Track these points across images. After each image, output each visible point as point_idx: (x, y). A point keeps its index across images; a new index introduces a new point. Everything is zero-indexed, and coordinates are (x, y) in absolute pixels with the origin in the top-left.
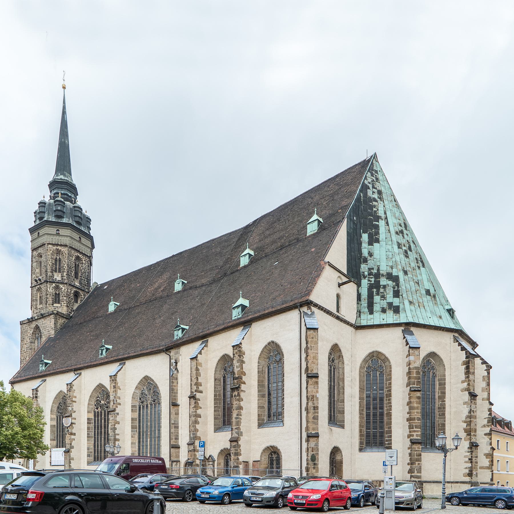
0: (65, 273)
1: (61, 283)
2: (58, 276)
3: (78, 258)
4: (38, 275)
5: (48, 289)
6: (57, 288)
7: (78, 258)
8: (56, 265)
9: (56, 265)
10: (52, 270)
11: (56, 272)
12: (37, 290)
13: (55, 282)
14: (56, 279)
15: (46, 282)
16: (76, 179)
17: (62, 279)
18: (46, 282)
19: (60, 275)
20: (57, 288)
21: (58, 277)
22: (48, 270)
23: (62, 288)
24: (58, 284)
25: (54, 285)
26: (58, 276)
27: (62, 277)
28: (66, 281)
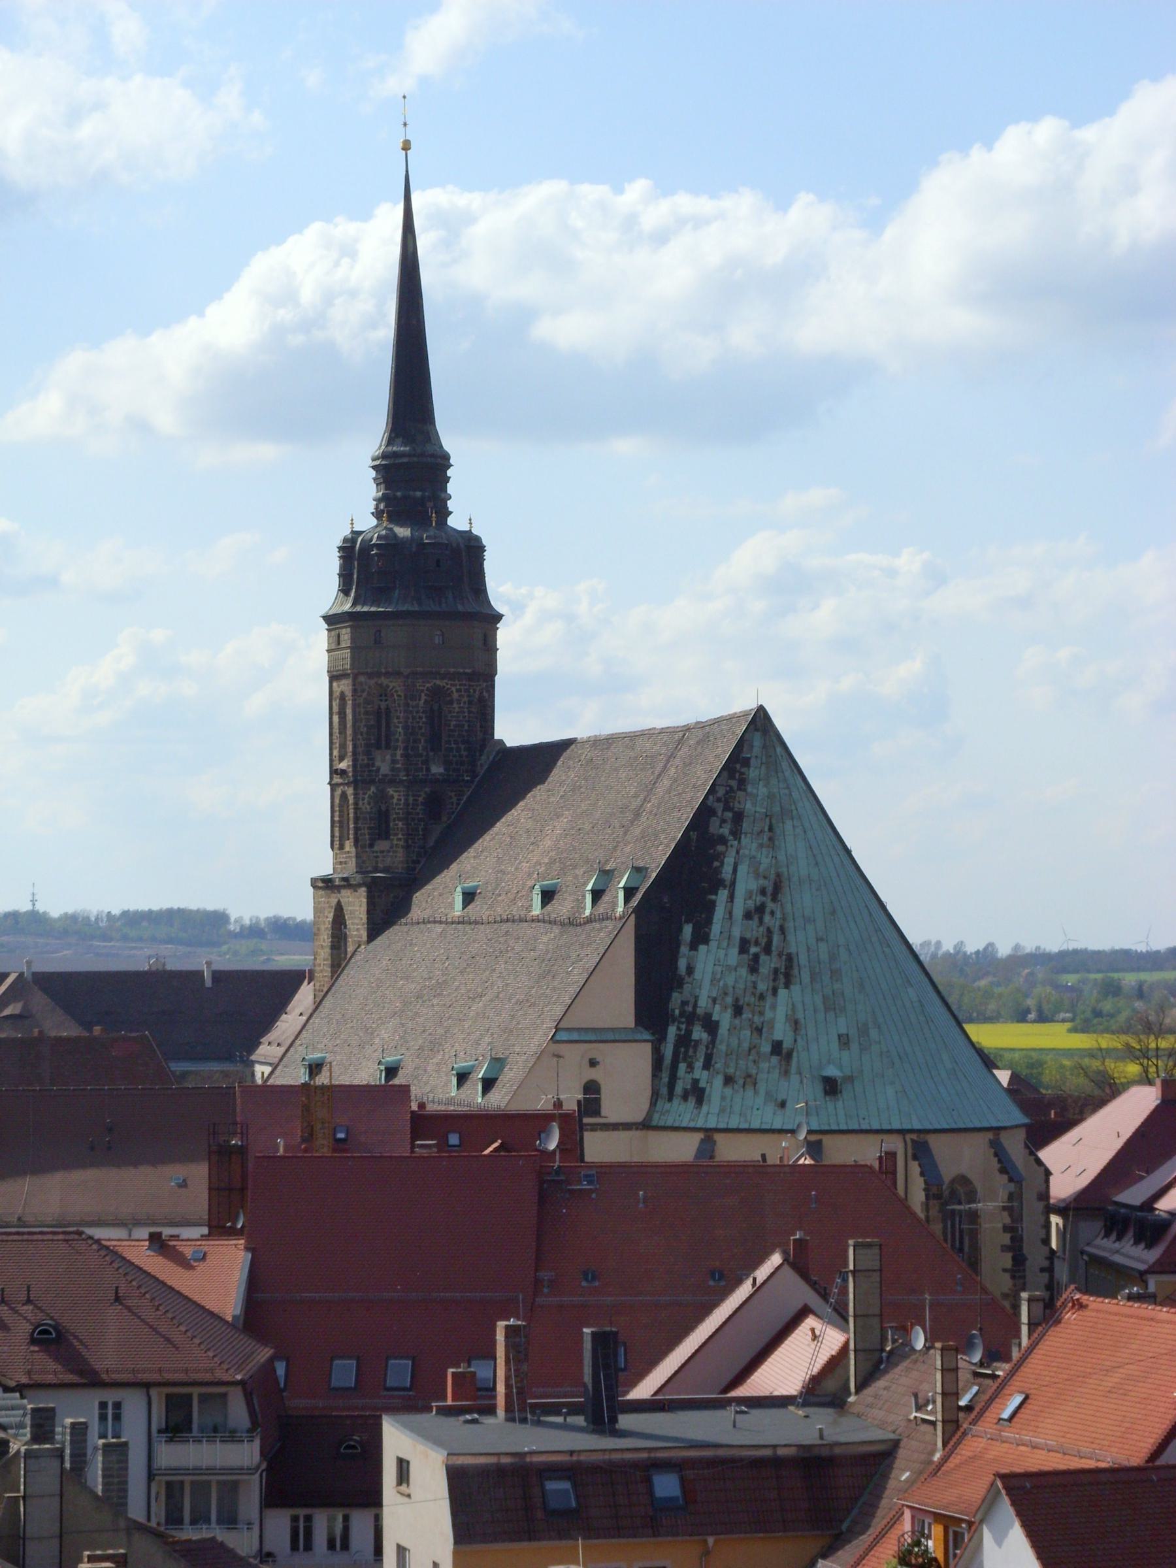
0: (399, 752)
2: (383, 761)
3: (437, 694)
5: (361, 802)
6: (382, 797)
7: (437, 694)
8: (379, 722)
9: (379, 728)
10: (367, 745)
11: (378, 747)
13: (372, 782)
14: (378, 770)
17: (392, 769)
19: (388, 757)
23: (392, 797)
26: (383, 761)
27: (394, 762)
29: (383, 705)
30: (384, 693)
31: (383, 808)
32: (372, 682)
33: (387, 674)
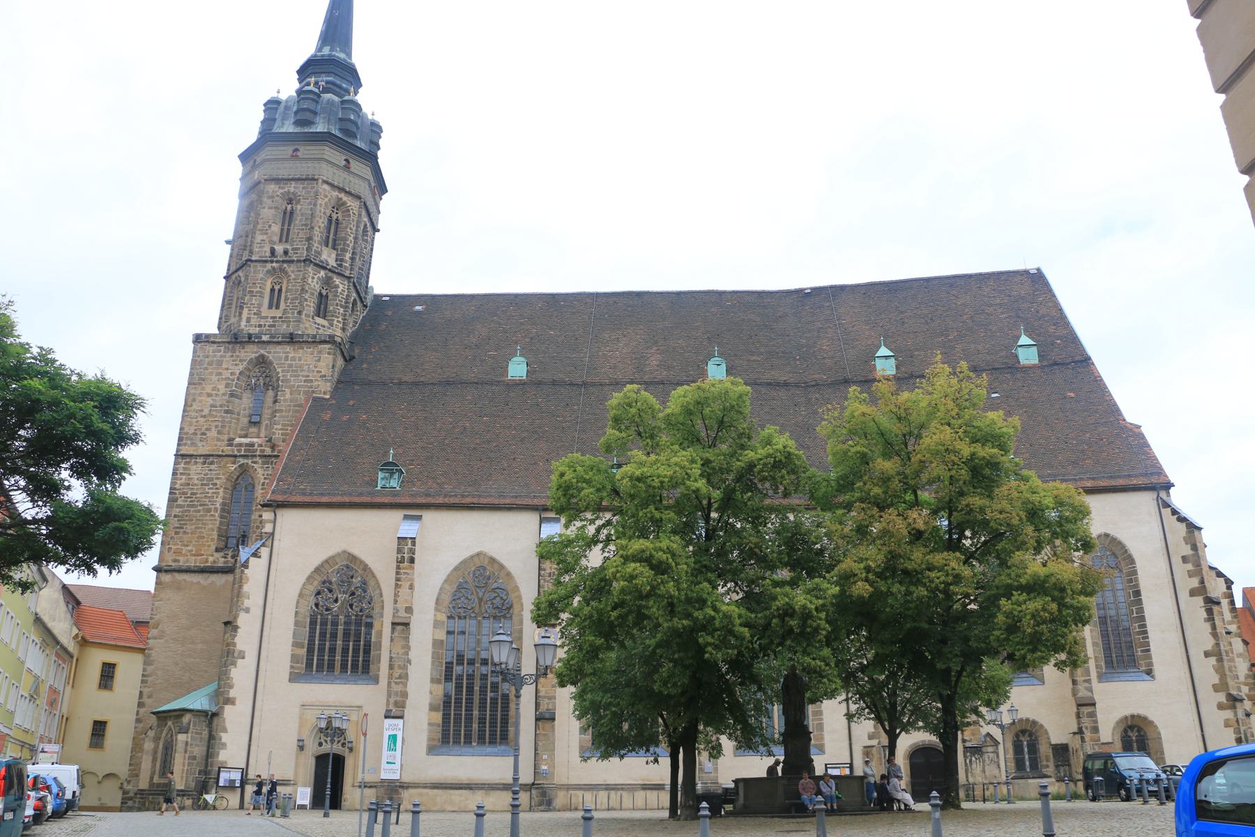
0: (348, 256)
1: (339, 274)
4: (276, 239)
12: (268, 272)
13: (324, 268)
15: (307, 261)
16: (360, 57)
18: (307, 261)
19: (334, 256)
20: (327, 282)
21: (329, 256)
22: (316, 238)
23: (337, 287)
24: (330, 274)
25: (322, 273)
27: (340, 260)
28: (347, 273)
29: (335, 217)
30: (339, 205)
31: (324, 292)
32: (335, 193)
33: (349, 193)
